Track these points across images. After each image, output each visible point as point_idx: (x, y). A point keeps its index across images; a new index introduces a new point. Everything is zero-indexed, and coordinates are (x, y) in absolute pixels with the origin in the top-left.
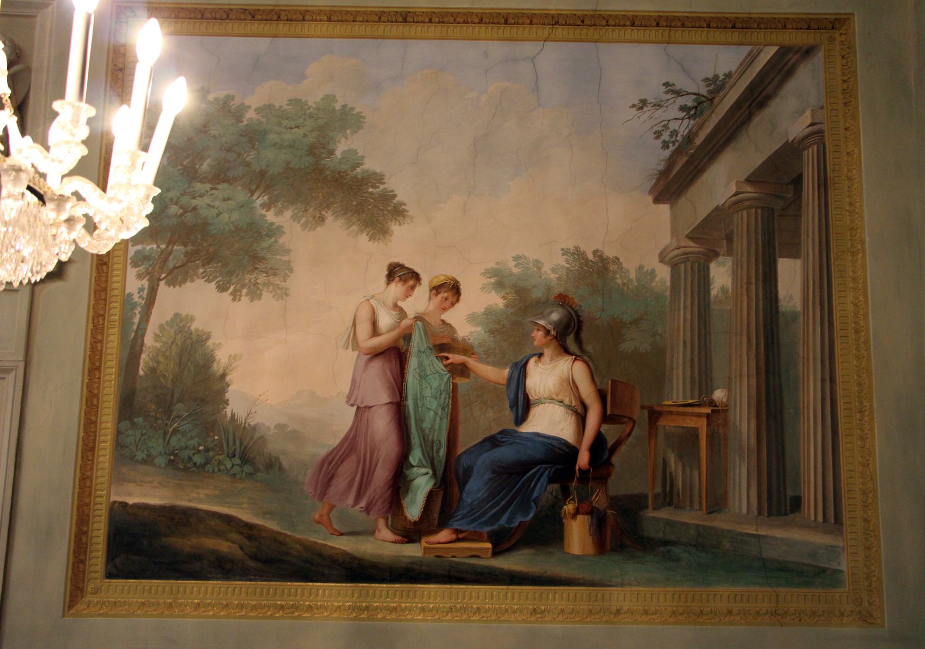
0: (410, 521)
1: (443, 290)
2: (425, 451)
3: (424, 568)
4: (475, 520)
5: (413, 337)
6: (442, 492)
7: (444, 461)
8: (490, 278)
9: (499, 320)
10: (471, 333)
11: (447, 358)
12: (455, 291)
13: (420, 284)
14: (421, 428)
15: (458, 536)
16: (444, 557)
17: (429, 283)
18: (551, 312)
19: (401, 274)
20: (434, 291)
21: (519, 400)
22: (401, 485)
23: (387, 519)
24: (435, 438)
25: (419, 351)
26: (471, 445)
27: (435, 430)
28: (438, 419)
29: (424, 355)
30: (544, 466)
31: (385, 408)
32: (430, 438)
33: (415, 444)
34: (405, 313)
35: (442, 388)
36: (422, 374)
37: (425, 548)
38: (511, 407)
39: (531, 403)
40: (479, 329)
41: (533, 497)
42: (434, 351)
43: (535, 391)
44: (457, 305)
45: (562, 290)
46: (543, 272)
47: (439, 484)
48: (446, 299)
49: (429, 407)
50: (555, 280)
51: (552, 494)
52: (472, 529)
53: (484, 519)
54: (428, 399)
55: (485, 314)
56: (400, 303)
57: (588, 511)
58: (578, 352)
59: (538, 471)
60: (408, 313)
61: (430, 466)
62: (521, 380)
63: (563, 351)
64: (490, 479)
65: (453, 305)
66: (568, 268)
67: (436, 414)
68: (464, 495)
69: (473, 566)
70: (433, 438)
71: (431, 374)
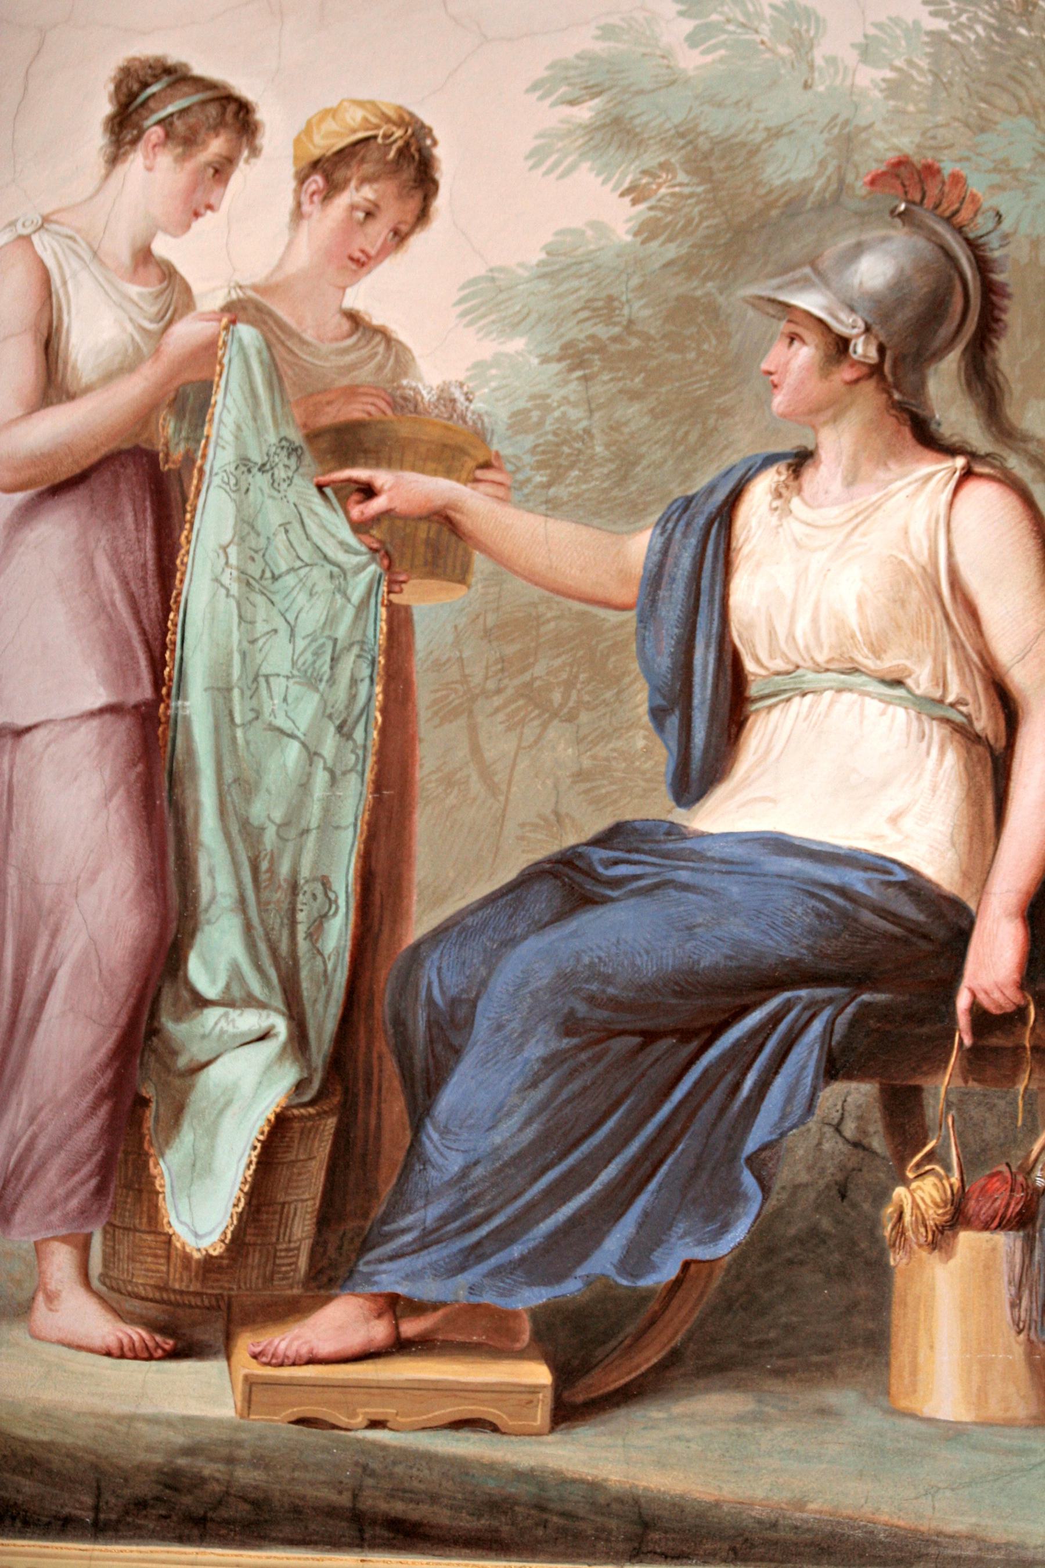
0: (187, 1258)
1: (354, 172)
2: (259, 931)
3: (247, 1476)
4: (475, 1254)
5: (218, 397)
6: (331, 1122)
7: (341, 978)
8: (572, 103)
9: (611, 299)
10: (480, 367)
11: (368, 491)
12: (409, 173)
13: (255, 152)
14: (245, 824)
15: (397, 1327)
16: (334, 1427)
17: (297, 141)
18: (858, 250)
19: (171, 109)
20: (317, 181)
21: (697, 679)
22: (148, 1091)
23: (84, 1248)
24: (305, 872)
25: (244, 463)
26: (462, 904)
27: (307, 831)
28: (321, 778)
29: (261, 480)
30: (803, 993)
31: (87, 734)
32: (284, 869)
33: (213, 899)
34: (187, 290)
35: (342, 631)
36: (255, 570)
37: (251, 1383)
38: (658, 715)
39: (753, 691)
40: (518, 344)
41: (751, 1145)
42: (308, 458)
43: (772, 633)
44: (419, 242)
45: (906, 143)
46: (819, 62)
47: (316, 1085)
48: (369, 214)
49: (281, 722)
50: (877, 94)
51: (838, 1129)
52: (463, 1296)
53: (516, 1251)
54: (278, 685)
55: (543, 276)
56: (163, 247)
57: (1014, 1209)
58: (978, 438)
59: (775, 1019)
60: (196, 288)
61: (278, 1002)
62: (705, 583)
63: (907, 432)
64: (551, 1062)
65: (400, 237)
66: (937, 37)
67: (312, 755)
68: (432, 1135)
69: (460, 1466)
70: (295, 871)
71: (293, 570)
